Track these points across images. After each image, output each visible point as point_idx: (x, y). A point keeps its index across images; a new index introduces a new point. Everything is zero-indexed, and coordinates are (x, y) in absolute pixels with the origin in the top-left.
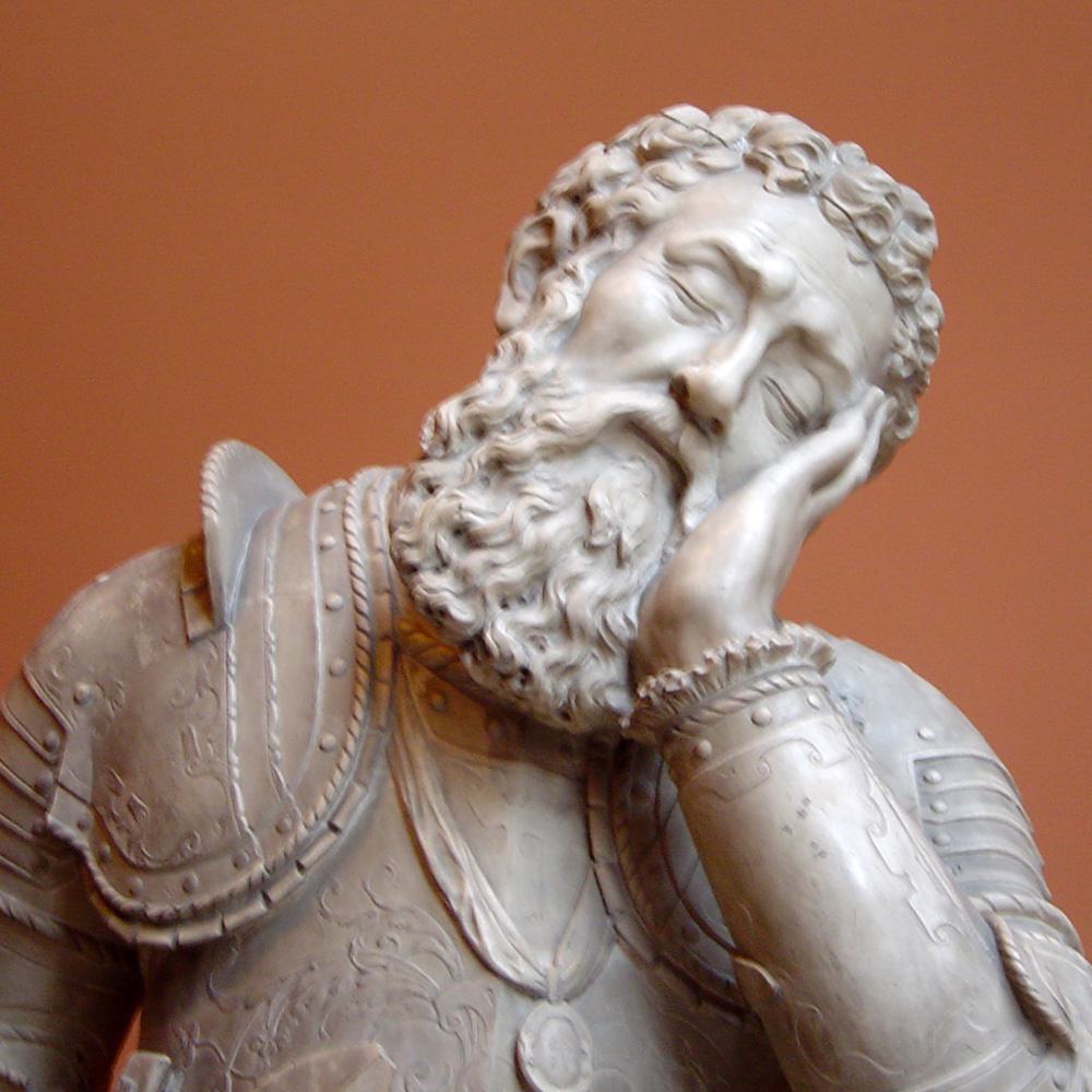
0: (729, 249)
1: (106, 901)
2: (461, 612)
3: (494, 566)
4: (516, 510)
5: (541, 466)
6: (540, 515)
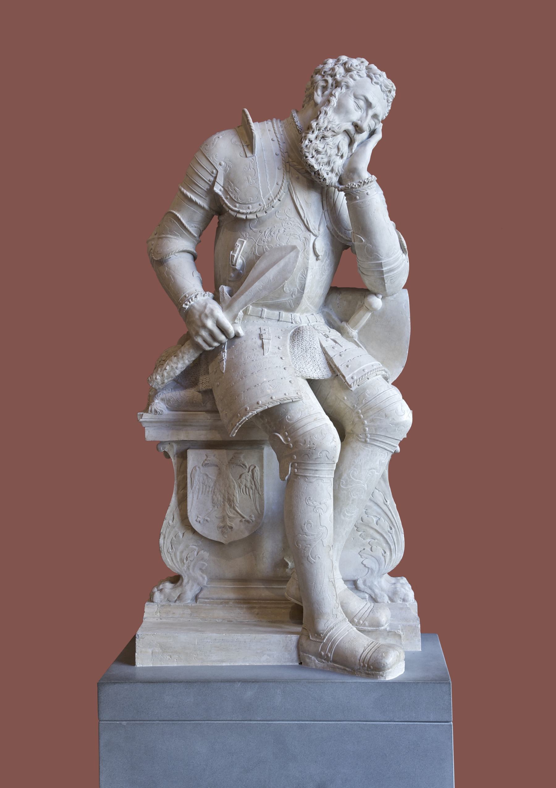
2: (316, 167)
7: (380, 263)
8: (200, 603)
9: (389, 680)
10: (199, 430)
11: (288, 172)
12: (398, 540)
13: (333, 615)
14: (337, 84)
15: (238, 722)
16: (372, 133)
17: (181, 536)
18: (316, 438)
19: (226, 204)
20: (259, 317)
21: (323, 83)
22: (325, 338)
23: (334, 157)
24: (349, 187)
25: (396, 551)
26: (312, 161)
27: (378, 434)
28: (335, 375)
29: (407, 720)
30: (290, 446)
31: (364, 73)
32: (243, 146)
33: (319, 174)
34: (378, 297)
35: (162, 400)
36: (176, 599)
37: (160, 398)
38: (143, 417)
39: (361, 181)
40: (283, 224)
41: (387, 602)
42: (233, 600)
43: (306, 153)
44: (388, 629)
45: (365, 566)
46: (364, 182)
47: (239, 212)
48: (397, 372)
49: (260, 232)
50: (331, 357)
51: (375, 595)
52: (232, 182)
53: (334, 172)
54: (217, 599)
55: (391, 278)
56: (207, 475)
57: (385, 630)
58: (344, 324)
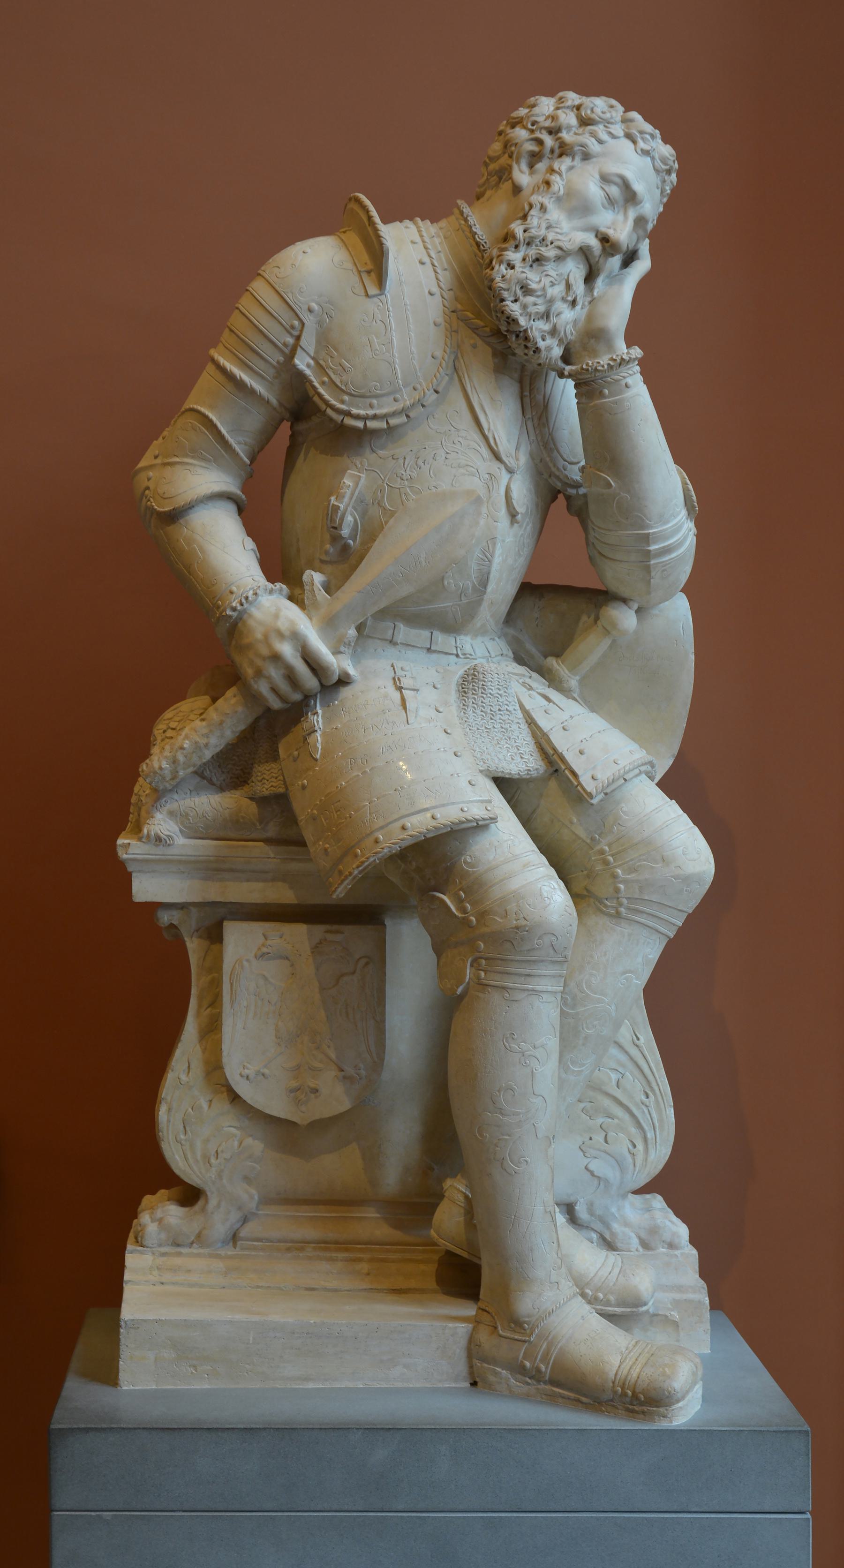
0: (627, 180)
1: (326, 403)
2: (523, 321)
3: (535, 304)
4: (546, 281)
5: (553, 263)
6: (553, 284)
7: (645, 534)
8: (242, 1249)
9: (677, 1426)
10: (248, 880)
11: (455, 331)
12: (661, 1120)
13: (551, 1283)
14: (564, 150)
15: (355, 1514)
16: (630, 258)
17: (205, 1106)
18: (529, 905)
19: (320, 396)
20: (386, 640)
21: (531, 144)
22: (525, 690)
23: (560, 306)
24: (590, 369)
25: (657, 1144)
26: (514, 309)
27: (646, 898)
28: (552, 770)
29: (717, 1509)
30: (471, 921)
31: (618, 129)
32: (359, 272)
33: (527, 339)
34: (630, 608)
35: (172, 814)
36: (192, 1240)
37: (166, 809)
38: (130, 851)
39: (614, 357)
40: (444, 443)
41: (637, 1250)
42: (314, 1243)
43: (502, 292)
44: (651, 1311)
45: (592, 1173)
46: (622, 359)
47: (348, 414)
48: (664, 765)
49: (393, 458)
50: (545, 731)
51: (613, 1234)
52: (336, 350)
53: (557, 335)
54: (279, 1241)
55: (663, 566)
56: (265, 978)
57: (647, 1312)
58: (552, 662)
